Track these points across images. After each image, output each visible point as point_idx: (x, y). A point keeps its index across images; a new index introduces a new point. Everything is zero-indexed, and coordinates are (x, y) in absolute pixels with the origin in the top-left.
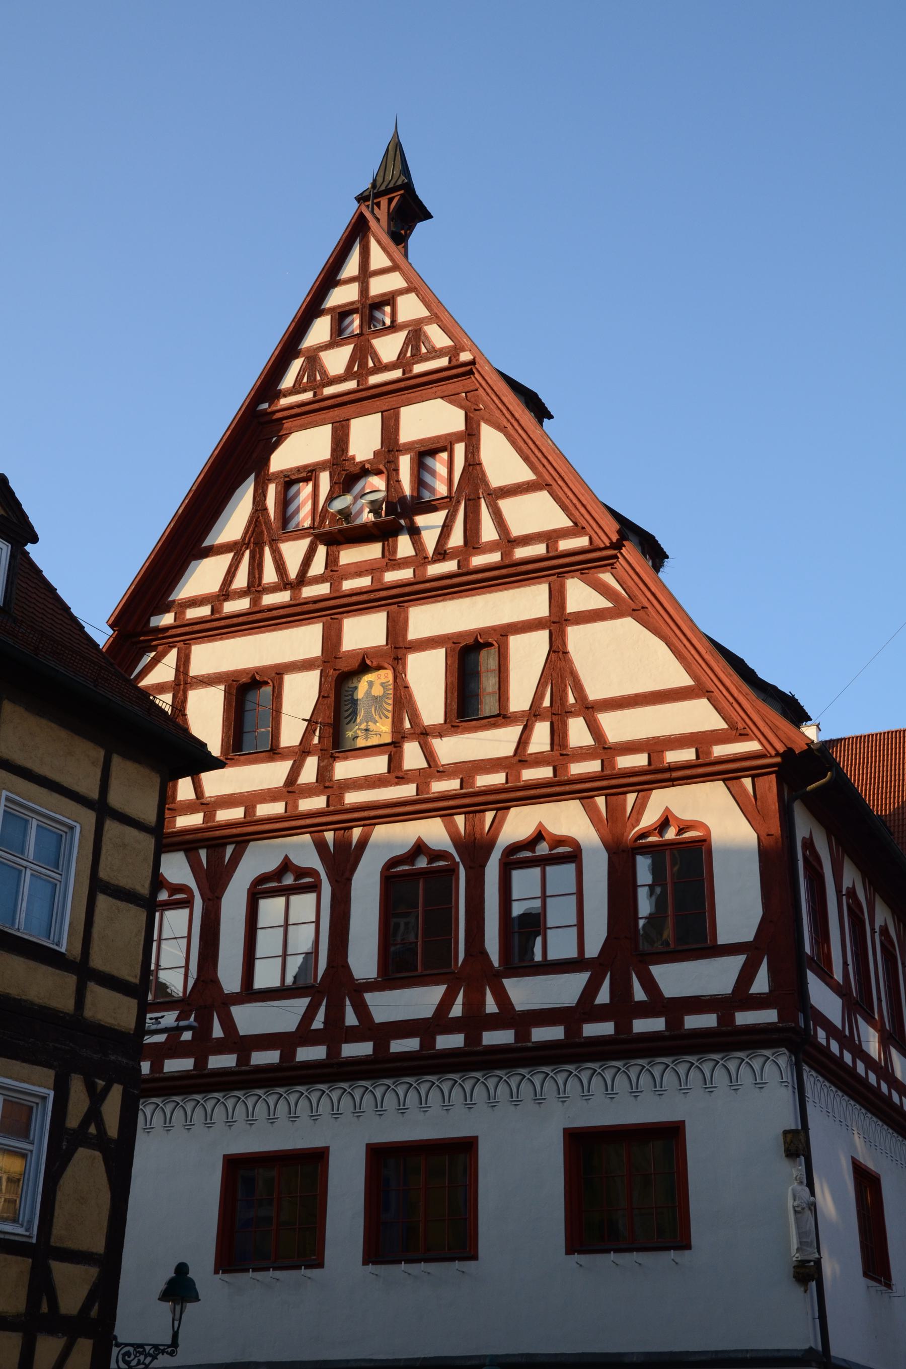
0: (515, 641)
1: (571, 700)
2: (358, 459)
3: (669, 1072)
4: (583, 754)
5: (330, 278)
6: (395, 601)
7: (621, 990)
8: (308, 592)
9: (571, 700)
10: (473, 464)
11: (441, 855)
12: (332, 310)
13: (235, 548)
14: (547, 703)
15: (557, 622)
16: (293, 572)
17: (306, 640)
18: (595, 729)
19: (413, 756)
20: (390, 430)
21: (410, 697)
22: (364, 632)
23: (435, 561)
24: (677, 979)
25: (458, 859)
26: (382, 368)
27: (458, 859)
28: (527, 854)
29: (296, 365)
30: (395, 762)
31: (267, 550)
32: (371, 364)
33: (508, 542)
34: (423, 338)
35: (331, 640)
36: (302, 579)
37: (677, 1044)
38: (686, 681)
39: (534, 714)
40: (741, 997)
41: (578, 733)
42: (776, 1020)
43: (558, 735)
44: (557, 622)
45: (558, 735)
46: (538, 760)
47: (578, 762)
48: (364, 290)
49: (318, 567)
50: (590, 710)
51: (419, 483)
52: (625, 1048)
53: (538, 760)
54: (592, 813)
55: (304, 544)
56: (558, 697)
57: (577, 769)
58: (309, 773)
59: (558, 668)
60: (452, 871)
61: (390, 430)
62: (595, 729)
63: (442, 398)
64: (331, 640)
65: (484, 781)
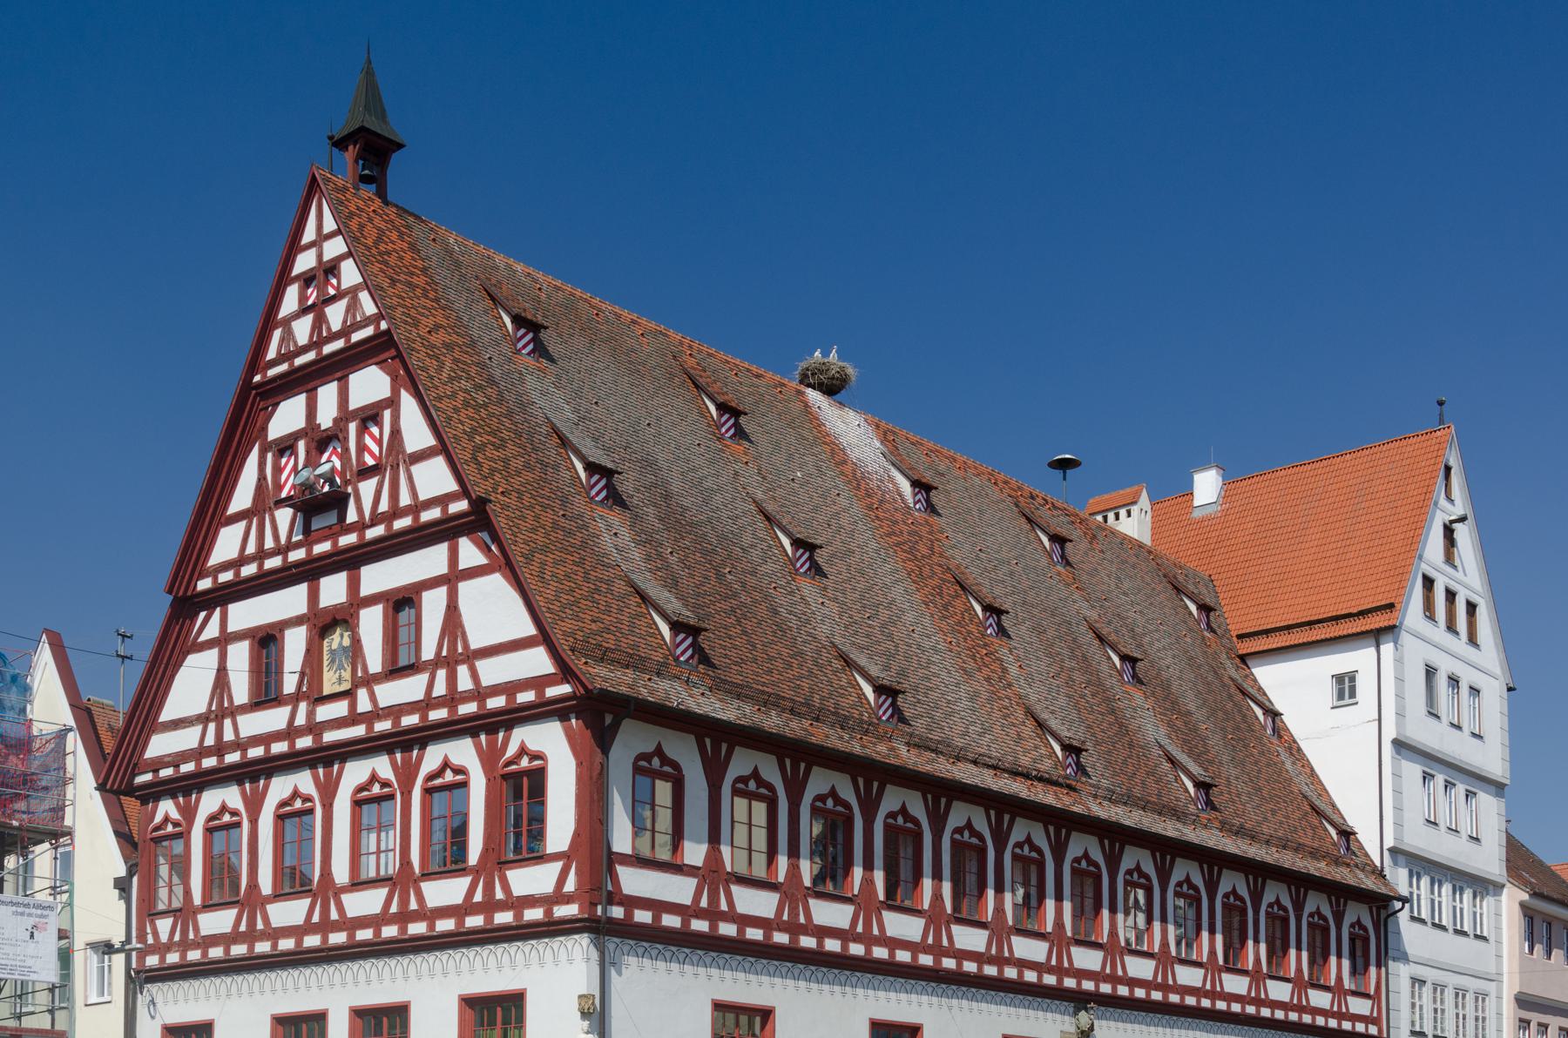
1: (460, 650)
6: (351, 561)
7: (489, 889)
11: (385, 784)
14: (444, 653)
15: (453, 578)
17: (292, 601)
19: (364, 705)
21: (361, 647)
22: (333, 589)
23: (372, 525)
30: (353, 706)
33: (417, 507)
35: (313, 596)
36: (291, 546)
38: (530, 630)
39: (437, 662)
43: (452, 679)
44: (453, 578)
45: (452, 679)
50: (472, 656)
54: (478, 746)
58: (301, 720)
59: (453, 622)
60: (391, 797)
64: (313, 596)
65: (410, 720)
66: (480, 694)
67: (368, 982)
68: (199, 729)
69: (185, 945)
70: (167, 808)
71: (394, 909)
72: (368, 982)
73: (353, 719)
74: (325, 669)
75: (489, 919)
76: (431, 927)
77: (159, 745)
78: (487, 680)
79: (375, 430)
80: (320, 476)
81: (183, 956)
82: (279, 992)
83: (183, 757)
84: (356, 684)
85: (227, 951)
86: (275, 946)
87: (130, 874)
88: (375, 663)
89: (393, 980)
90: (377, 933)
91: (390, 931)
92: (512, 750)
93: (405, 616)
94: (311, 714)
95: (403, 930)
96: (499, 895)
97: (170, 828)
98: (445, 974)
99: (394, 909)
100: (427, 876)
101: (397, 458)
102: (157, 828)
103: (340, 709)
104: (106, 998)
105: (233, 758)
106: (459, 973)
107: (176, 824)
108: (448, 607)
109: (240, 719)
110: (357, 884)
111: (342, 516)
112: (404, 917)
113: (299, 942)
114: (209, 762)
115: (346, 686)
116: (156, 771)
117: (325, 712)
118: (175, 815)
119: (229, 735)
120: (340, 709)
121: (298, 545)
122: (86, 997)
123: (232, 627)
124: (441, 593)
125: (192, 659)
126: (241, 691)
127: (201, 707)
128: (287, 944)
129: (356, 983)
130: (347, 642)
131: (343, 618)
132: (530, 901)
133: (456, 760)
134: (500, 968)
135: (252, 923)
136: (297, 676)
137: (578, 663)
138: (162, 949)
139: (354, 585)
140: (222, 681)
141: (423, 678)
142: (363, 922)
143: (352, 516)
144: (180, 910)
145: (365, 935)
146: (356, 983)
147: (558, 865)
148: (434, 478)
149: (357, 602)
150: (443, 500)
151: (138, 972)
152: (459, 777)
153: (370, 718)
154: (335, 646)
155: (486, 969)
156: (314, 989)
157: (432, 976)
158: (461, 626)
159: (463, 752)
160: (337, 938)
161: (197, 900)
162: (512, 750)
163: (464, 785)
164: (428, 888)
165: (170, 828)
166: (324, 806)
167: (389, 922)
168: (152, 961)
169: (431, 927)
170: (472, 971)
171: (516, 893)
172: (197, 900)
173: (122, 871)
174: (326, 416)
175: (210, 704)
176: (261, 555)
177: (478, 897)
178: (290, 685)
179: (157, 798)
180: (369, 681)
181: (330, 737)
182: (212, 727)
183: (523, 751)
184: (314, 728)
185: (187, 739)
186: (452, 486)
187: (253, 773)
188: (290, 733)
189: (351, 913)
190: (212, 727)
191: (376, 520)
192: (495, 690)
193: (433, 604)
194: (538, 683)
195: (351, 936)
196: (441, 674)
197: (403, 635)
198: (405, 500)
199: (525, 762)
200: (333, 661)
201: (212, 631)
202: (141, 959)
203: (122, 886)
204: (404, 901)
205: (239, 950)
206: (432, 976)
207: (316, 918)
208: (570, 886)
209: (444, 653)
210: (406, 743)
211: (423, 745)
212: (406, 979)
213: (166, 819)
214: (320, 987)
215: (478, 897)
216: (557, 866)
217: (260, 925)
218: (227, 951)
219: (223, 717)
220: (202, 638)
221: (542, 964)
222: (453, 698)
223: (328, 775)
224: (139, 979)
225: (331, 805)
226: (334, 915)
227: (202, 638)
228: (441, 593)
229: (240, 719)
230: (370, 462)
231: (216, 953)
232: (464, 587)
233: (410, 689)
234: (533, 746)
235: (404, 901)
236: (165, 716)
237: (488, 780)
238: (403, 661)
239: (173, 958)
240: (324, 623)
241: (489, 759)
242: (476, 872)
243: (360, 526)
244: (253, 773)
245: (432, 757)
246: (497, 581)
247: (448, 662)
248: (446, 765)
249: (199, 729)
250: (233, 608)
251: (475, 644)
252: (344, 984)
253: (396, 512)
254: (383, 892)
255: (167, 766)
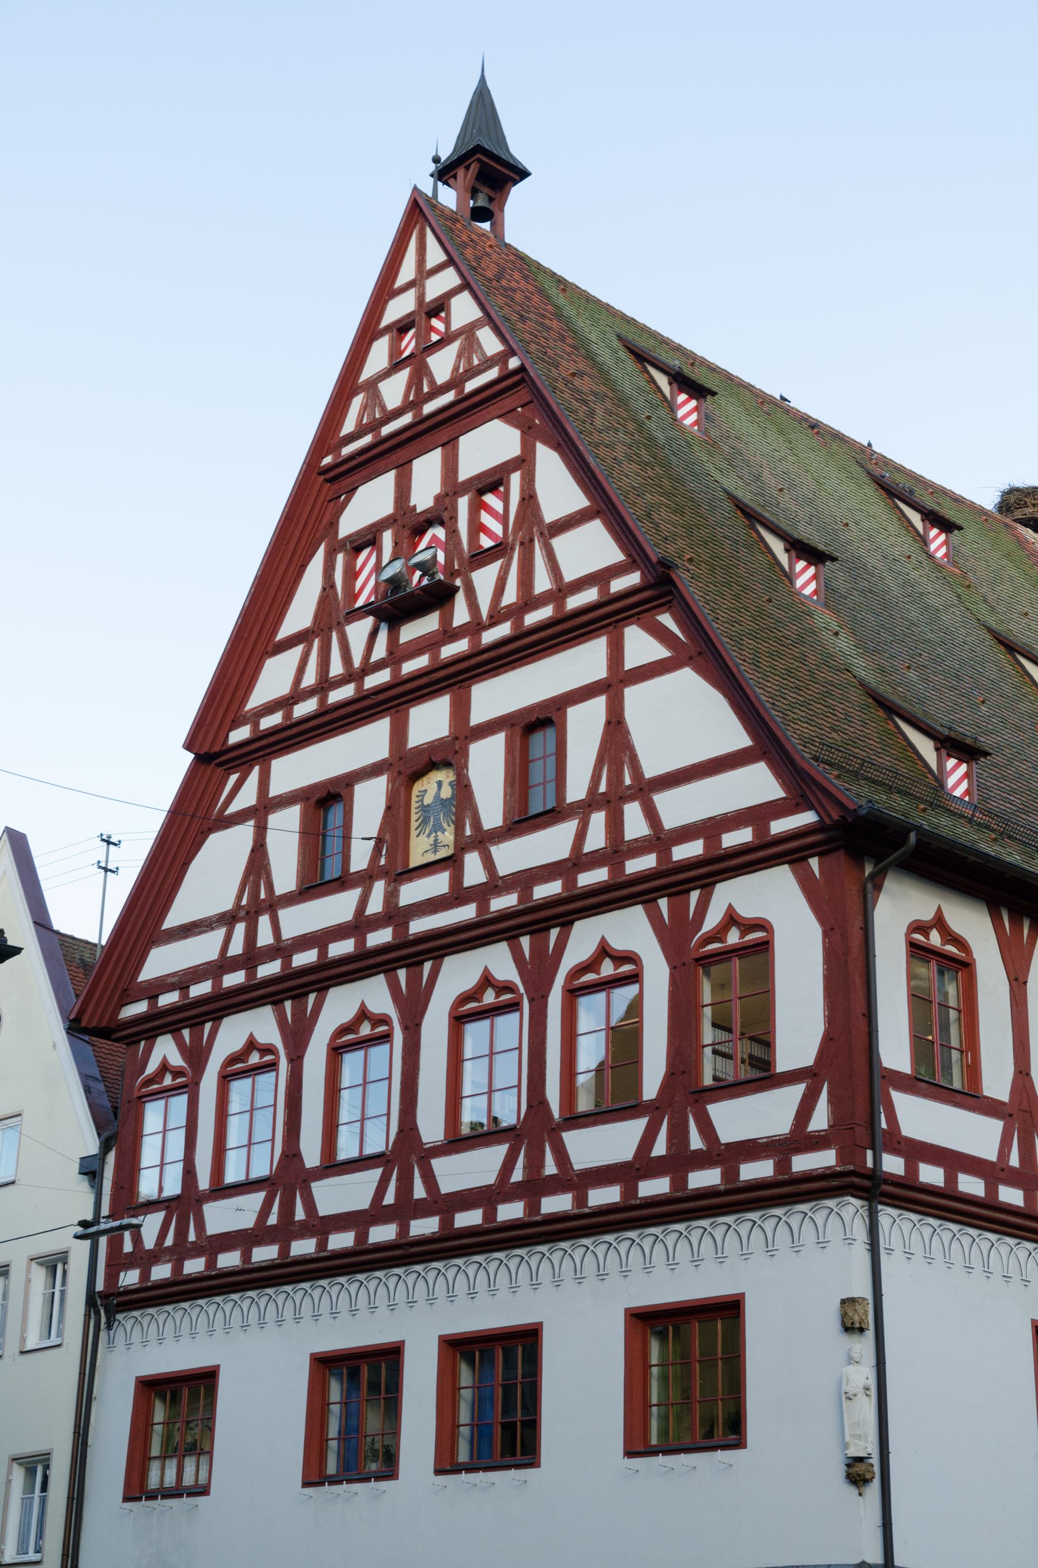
0: (574, 714)
1: (628, 781)
2: (419, 510)
3: (729, 1232)
4: (639, 848)
5: (385, 289)
6: (455, 679)
7: (678, 1136)
8: (372, 681)
9: (628, 781)
10: (529, 498)
12: (388, 329)
13: (301, 638)
14: (603, 788)
15: (615, 684)
16: (357, 662)
17: (371, 742)
18: (651, 814)
19: (474, 872)
20: (450, 466)
22: (429, 721)
24: (738, 1119)
25: (522, 990)
26: (438, 391)
27: (522, 990)
28: (590, 977)
29: (357, 402)
31: (334, 635)
32: (426, 389)
33: (562, 590)
34: (475, 346)
35: (399, 734)
37: (736, 1200)
40: (801, 1139)
41: (635, 824)
42: (834, 1163)
43: (615, 825)
44: (615, 684)
45: (615, 825)
46: (595, 860)
47: (633, 858)
48: (420, 298)
49: (380, 652)
50: (646, 790)
51: (477, 528)
52: (684, 1208)
53: (595, 860)
55: (369, 621)
56: (616, 778)
57: (635, 866)
58: (375, 905)
61: (450, 466)
62: (651, 814)
63: (499, 417)
64: (399, 734)
65: (544, 891)
66: (661, 840)
67: (472, 1295)
68: (220, 933)
69: (181, 1252)
70: (166, 1050)
71: (517, 1175)
72: (472, 1295)
73: (457, 896)
74: (413, 833)
75: (679, 1182)
76: (581, 1200)
77: (161, 962)
78: (670, 821)
79: (492, 500)
80: (419, 566)
81: (178, 1268)
82: (326, 1317)
83: (196, 974)
84: (462, 847)
85: (246, 1256)
86: (322, 1244)
87: (105, 1148)
88: (492, 812)
89: (514, 1289)
90: (490, 1215)
91: (511, 1211)
92: (712, 920)
93: (541, 742)
94: (391, 896)
95: (533, 1207)
96: (696, 1142)
97: (168, 1081)
98: (601, 1276)
99: (517, 1175)
100: (575, 1120)
101: (533, 529)
102: (149, 1081)
103: (438, 884)
104: (54, 1340)
105: (269, 969)
106: (625, 1273)
107: (177, 1073)
108: (608, 723)
109: (283, 914)
110: (458, 1141)
111: (446, 619)
112: (535, 1187)
113: (362, 1236)
114: (234, 979)
115: (443, 853)
116: (153, 998)
117: (411, 893)
118: (176, 1060)
119: (265, 937)
120: (438, 884)
121: (380, 666)
122: (23, 1340)
123: (276, 789)
124: (599, 703)
125: (215, 841)
126: (285, 876)
127: (226, 904)
128: (342, 1241)
129: (451, 1297)
130: (446, 792)
131: (448, 755)
132: (751, 1149)
133: (618, 944)
134: (696, 1262)
135: (287, 1210)
136: (372, 843)
137: (830, 778)
138: (144, 1259)
139: (461, 710)
140: (258, 863)
141: (568, 829)
142: (465, 1199)
143: (461, 615)
144: (177, 1198)
145: (469, 1219)
146: (451, 1297)
147: (796, 1092)
148: (588, 549)
149: (465, 732)
150: (601, 577)
151: (105, 1296)
152: (627, 968)
153: (481, 894)
154: (428, 800)
155: (671, 1261)
156: (383, 1311)
157: (579, 1280)
158: (629, 748)
159: (631, 929)
160: (425, 1226)
161: (204, 1183)
162: (712, 920)
163: (634, 978)
164: (571, 1139)
165: (168, 1081)
166: (405, 1028)
167: (508, 1198)
168: (130, 1278)
169: (581, 1200)
170: (648, 1269)
171: (724, 1140)
172: (204, 1183)
173: (92, 1146)
174: (425, 490)
175: (239, 897)
176: (325, 683)
177: (660, 1148)
178: (360, 858)
179: (151, 1036)
180: (483, 841)
181: (418, 926)
182: (240, 928)
183: (731, 919)
184: (396, 915)
185: (205, 948)
186: (615, 555)
187: (297, 990)
188: (360, 925)
189: (446, 1186)
190: (240, 928)
191: (496, 618)
192: (686, 834)
193: (585, 724)
194: (756, 816)
195: (447, 1222)
196: (598, 820)
197: (540, 772)
198: (542, 583)
199: (733, 937)
200: (425, 822)
201: (247, 797)
202: (112, 1276)
203: (91, 1171)
204: (535, 1163)
205: (265, 1254)
206: (579, 1280)
207: (389, 1199)
208: (820, 1120)
209: (603, 788)
210: (537, 923)
211: (566, 923)
212: (535, 1286)
213: (165, 1067)
214: (392, 1307)
215: (660, 1148)
216: (796, 1092)
217: (300, 1214)
218: (246, 1256)
219: (258, 913)
220: (232, 809)
221: (770, 1250)
222: (618, 850)
223: (414, 980)
224: (108, 1305)
225: (418, 1025)
226: (419, 1191)
227: (232, 809)
228: (599, 703)
229: (283, 914)
230: (486, 542)
231: (230, 1260)
232: (633, 695)
233: (553, 843)
234: (746, 911)
235: (535, 1163)
236: (173, 919)
237: (673, 968)
238: (536, 807)
239: (161, 1272)
240: (407, 767)
241: (674, 937)
242: (654, 1110)
243: (475, 627)
244: (297, 990)
245: (582, 940)
246: (687, 680)
247: (608, 802)
248: (604, 951)
249: (220, 933)
250: (278, 765)
251: (651, 770)
252: (431, 1300)
253: (528, 602)
254: (498, 1152)
255: (170, 988)
